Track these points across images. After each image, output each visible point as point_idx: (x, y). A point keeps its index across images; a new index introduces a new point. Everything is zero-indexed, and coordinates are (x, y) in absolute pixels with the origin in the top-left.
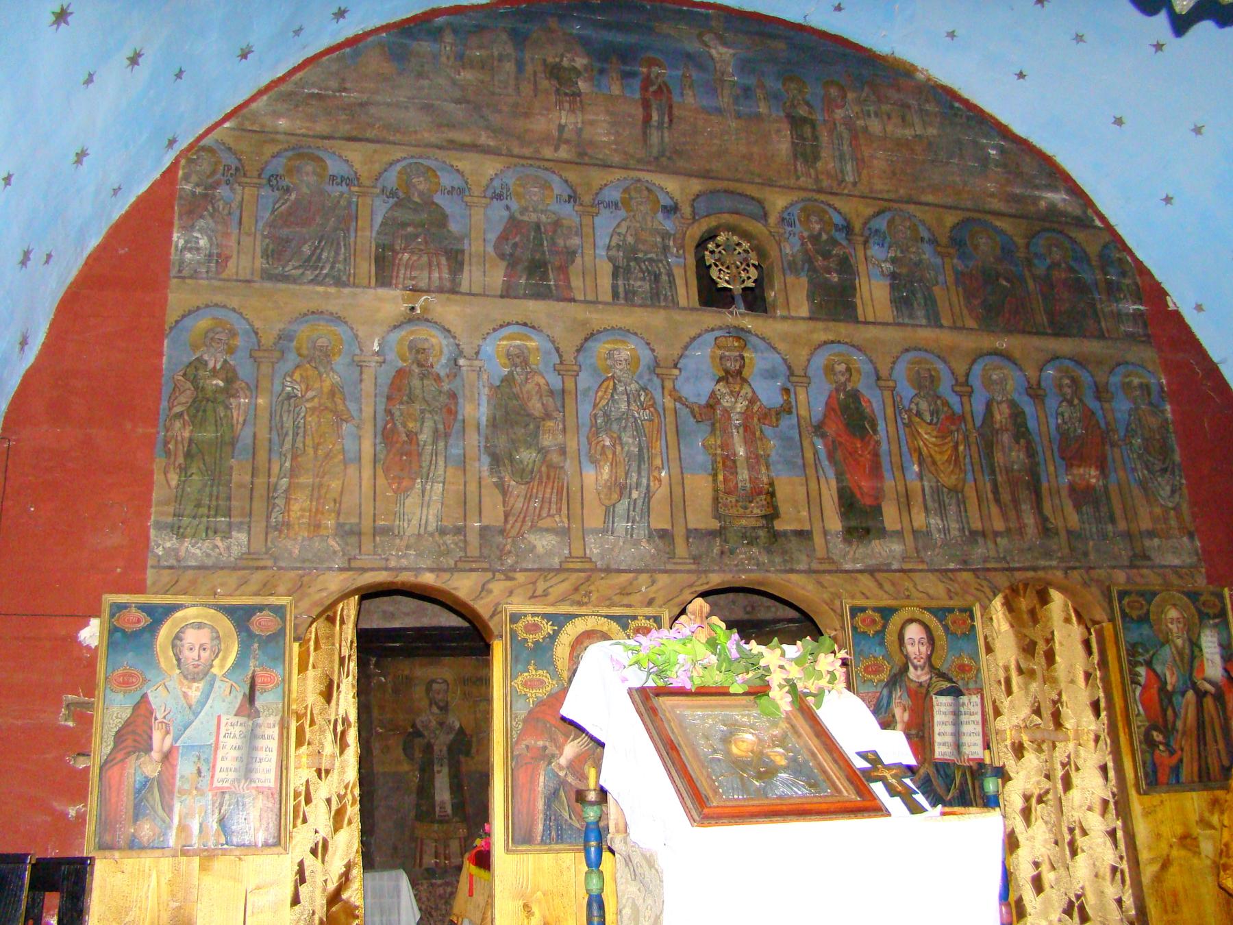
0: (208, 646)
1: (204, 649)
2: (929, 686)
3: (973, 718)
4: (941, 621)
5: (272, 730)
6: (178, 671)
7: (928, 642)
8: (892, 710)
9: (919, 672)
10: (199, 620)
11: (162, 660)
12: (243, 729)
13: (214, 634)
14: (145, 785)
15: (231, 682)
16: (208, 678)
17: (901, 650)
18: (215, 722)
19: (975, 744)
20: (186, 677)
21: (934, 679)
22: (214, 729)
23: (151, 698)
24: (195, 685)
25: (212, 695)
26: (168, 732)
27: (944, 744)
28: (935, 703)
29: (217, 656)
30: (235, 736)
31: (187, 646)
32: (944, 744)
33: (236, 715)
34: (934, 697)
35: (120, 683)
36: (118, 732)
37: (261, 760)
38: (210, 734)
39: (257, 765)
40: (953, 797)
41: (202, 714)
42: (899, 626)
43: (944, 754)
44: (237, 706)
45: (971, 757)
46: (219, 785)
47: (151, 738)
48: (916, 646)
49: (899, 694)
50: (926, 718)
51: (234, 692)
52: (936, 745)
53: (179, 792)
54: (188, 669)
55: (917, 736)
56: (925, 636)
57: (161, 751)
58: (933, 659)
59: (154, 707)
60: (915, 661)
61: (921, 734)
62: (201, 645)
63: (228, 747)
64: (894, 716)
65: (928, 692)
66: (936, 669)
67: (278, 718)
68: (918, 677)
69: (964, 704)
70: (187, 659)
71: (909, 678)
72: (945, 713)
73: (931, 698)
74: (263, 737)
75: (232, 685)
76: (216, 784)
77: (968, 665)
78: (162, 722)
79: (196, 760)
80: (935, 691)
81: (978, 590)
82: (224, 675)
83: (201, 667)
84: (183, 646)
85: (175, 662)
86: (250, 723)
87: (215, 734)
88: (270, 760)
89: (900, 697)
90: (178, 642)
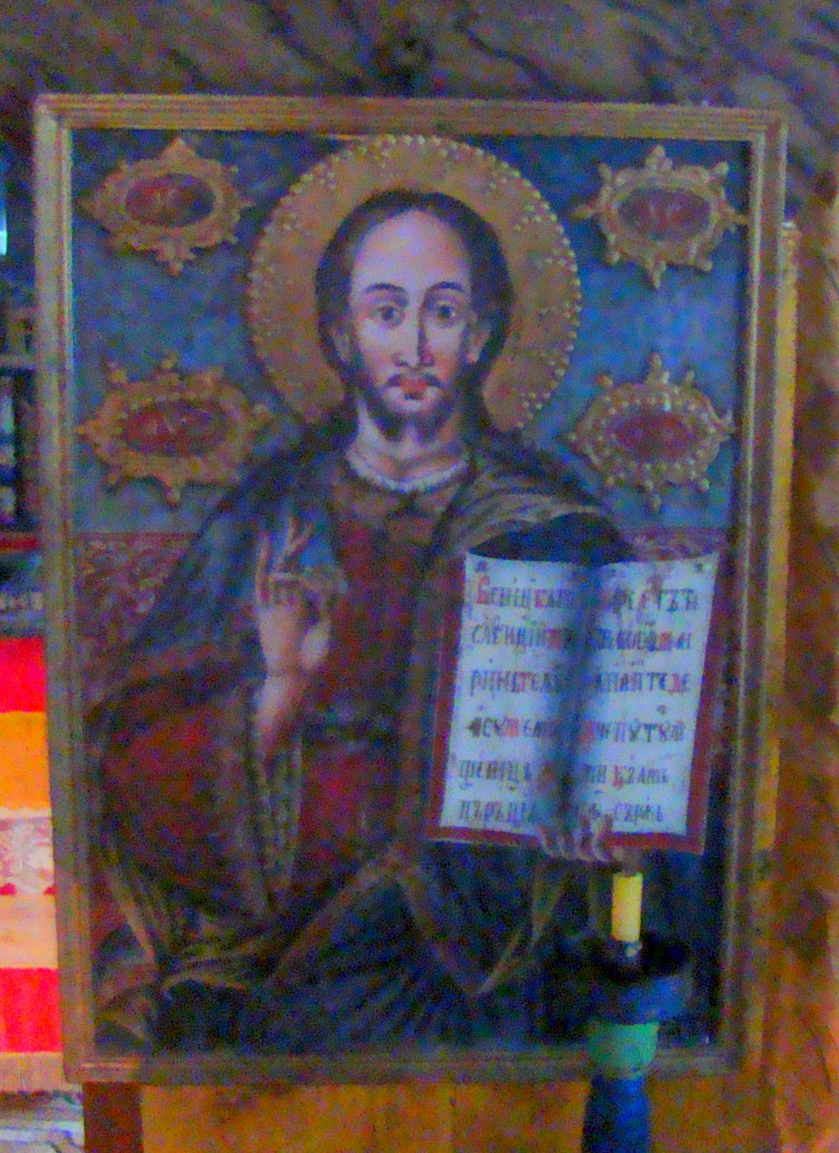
2: (453, 511)
3: (656, 661)
4: (563, 210)
7: (476, 305)
8: (246, 615)
9: (408, 447)
17: (326, 344)
19: (650, 775)
21: (486, 481)
27: (494, 770)
28: (471, 590)
32: (494, 770)
34: (470, 564)
40: (508, 988)
42: (324, 235)
43: (492, 809)
45: (620, 826)
48: (409, 327)
49: (289, 548)
50: (417, 659)
52: (452, 771)
55: (361, 729)
56: (458, 274)
58: (488, 390)
60: (395, 395)
61: (381, 724)
64: (252, 641)
65: (441, 533)
66: (494, 433)
68: (402, 469)
69: (621, 597)
71: (351, 475)
72: (518, 638)
73: (456, 572)
77: (673, 420)
80: (483, 536)
81: (805, 48)
89: (293, 563)
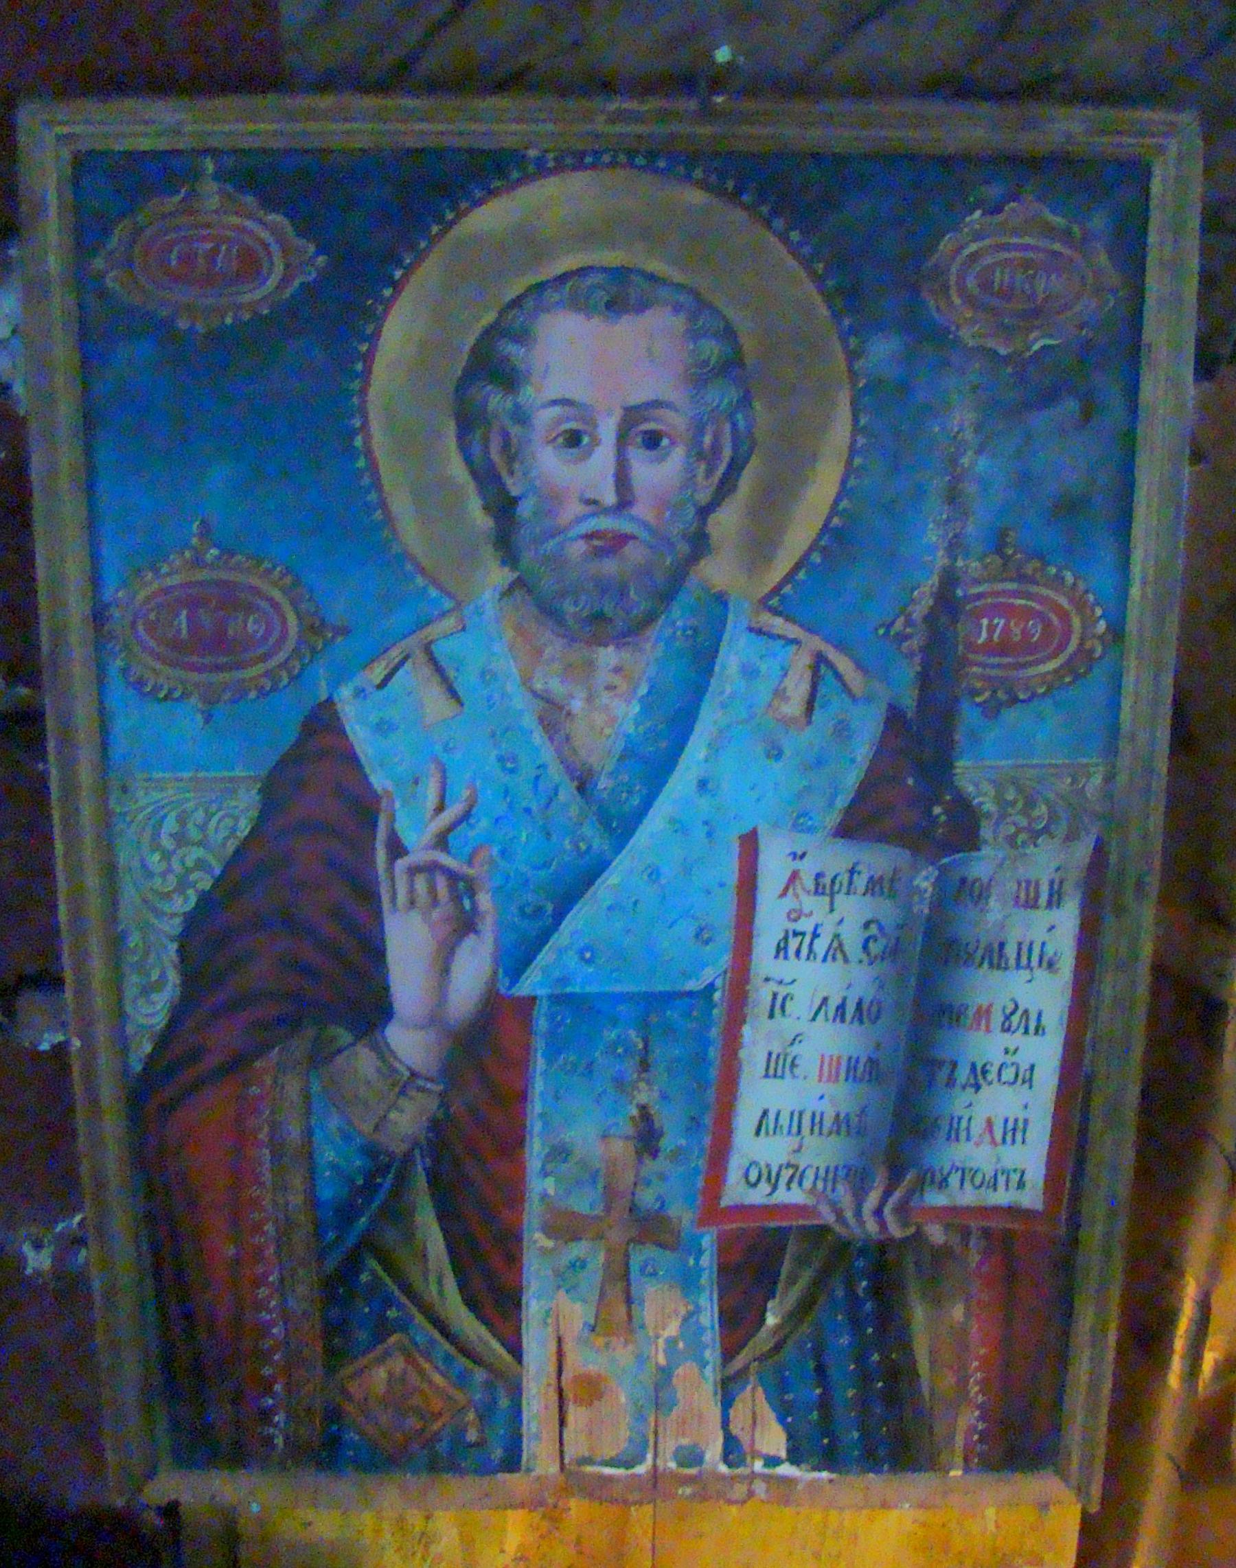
0: (676, 421)
1: (652, 441)
5: (1042, 917)
6: (500, 576)
10: (613, 258)
11: (401, 504)
12: (886, 910)
13: (711, 349)
14: (370, 1187)
15: (817, 643)
16: (679, 613)
18: (730, 869)
20: (549, 612)
22: (724, 908)
23: (359, 734)
24: (607, 656)
25: (709, 718)
26: (466, 925)
29: (726, 487)
30: (837, 950)
31: (547, 416)
33: (847, 830)
35: (176, 645)
36: (191, 922)
37: (979, 1076)
38: (703, 935)
39: (959, 1102)
41: (655, 823)
44: (852, 779)
46: (758, 1196)
47: (378, 954)
51: (834, 705)
53: (549, 1230)
54: (557, 561)
57: (434, 1019)
59: (378, 781)
62: (632, 416)
63: (800, 1007)
67: (1082, 851)
70: (552, 500)
74: (995, 956)
75: (820, 660)
76: (735, 1192)
78: (432, 868)
79: (629, 1067)
82: (766, 603)
83: (634, 554)
84: (521, 417)
85: (478, 516)
86: (925, 881)
87: (726, 936)
88: (1026, 1078)
90: (497, 402)
